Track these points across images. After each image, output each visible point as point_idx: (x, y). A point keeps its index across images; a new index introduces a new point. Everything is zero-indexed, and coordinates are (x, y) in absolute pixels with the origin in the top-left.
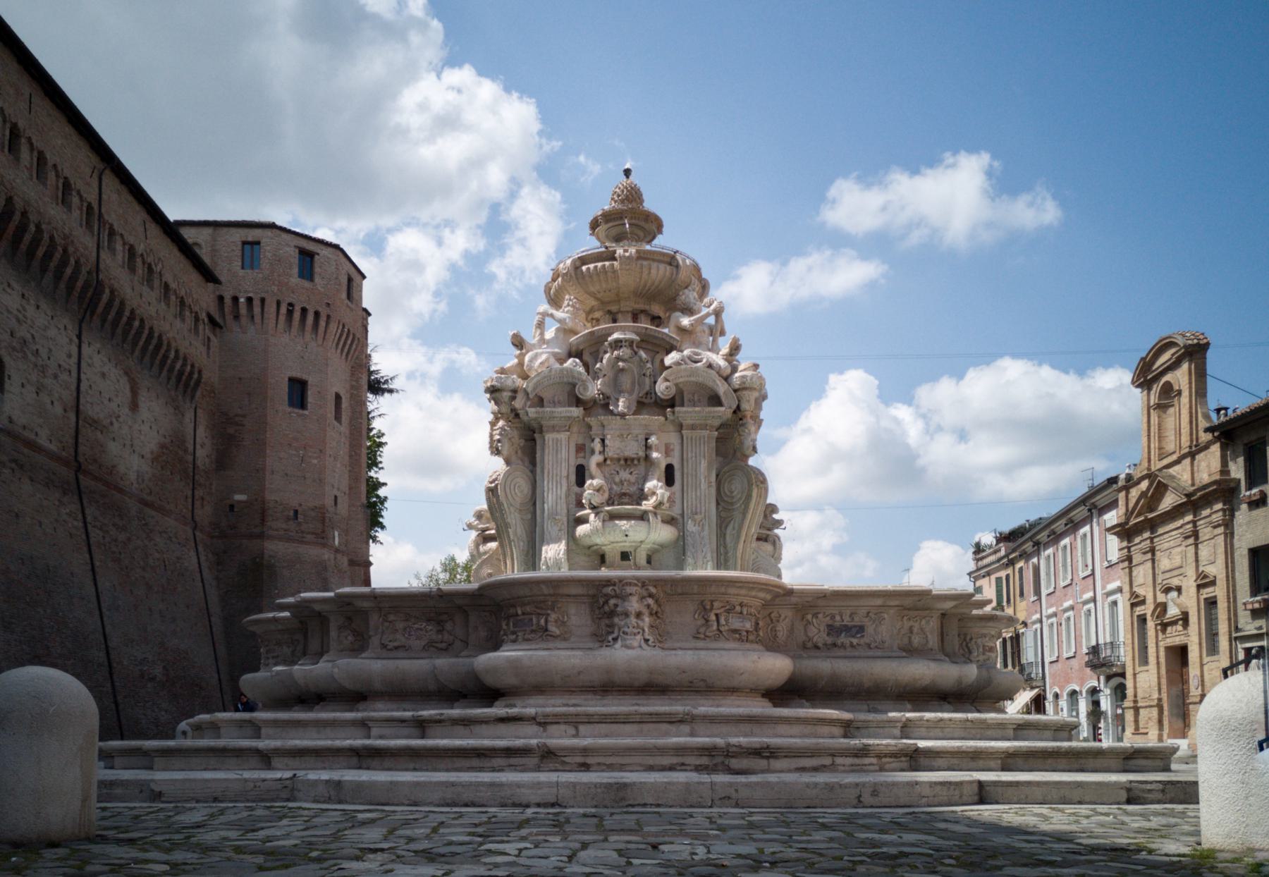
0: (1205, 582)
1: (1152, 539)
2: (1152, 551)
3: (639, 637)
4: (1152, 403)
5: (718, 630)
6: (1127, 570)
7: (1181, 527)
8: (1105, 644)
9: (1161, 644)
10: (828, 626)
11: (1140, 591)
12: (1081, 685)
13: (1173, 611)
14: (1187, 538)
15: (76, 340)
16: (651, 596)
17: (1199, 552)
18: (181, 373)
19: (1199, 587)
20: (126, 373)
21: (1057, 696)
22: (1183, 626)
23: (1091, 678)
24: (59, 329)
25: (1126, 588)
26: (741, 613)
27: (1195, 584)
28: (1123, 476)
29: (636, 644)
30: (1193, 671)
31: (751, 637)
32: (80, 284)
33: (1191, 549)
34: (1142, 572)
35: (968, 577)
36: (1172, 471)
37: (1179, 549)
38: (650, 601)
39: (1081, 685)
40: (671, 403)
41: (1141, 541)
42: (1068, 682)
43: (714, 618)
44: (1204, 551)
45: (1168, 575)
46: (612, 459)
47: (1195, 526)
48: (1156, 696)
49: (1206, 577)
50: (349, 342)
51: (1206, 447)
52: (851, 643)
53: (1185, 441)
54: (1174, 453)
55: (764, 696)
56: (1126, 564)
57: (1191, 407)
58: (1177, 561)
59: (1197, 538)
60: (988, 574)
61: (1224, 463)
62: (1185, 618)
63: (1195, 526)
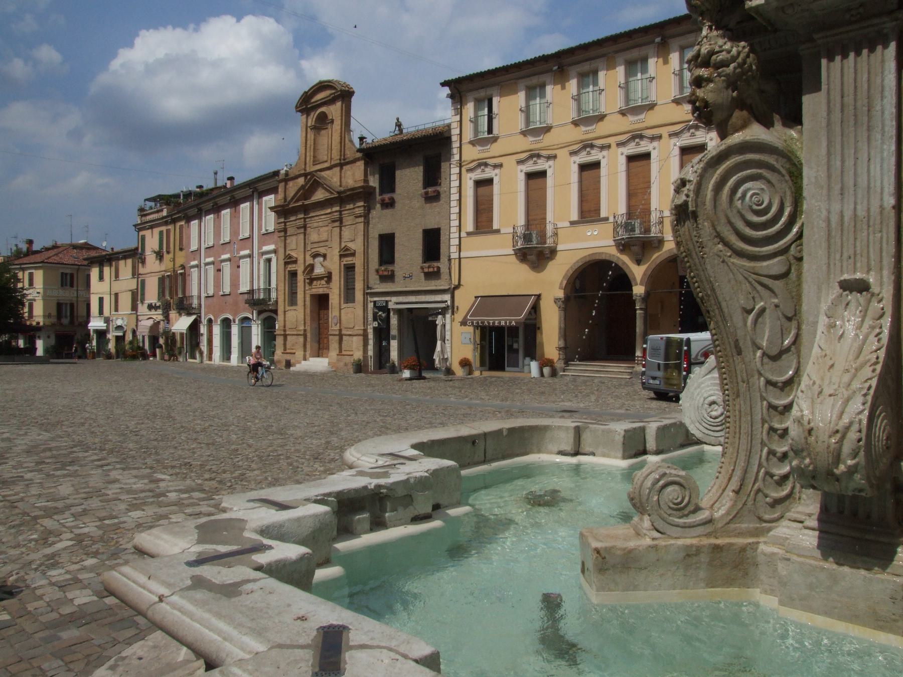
0: (346, 253)
1: (305, 219)
2: (305, 227)
4: (309, 124)
6: (283, 238)
7: (330, 213)
8: (259, 289)
9: (307, 292)
11: (294, 254)
12: (235, 315)
13: (319, 270)
14: (334, 221)
17: (342, 233)
19: (341, 256)
21: (210, 321)
22: (326, 282)
23: (244, 310)
25: (281, 251)
27: (338, 254)
28: (283, 172)
30: (333, 312)
33: (338, 230)
34: (294, 242)
35: (134, 228)
36: (323, 174)
37: (326, 229)
39: (235, 315)
41: (295, 221)
42: (223, 311)
44: (347, 233)
45: (315, 245)
47: (341, 214)
48: (302, 328)
49: (347, 250)
51: (354, 161)
53: (336, 155)
54: (326, 161)
56: (282, 234)
57: (341, 133)
58: (324, 236)
59: (341, 222)
60: (152, 227)
61: (366, 175)
62: (329, 277)
63: (341, 214)
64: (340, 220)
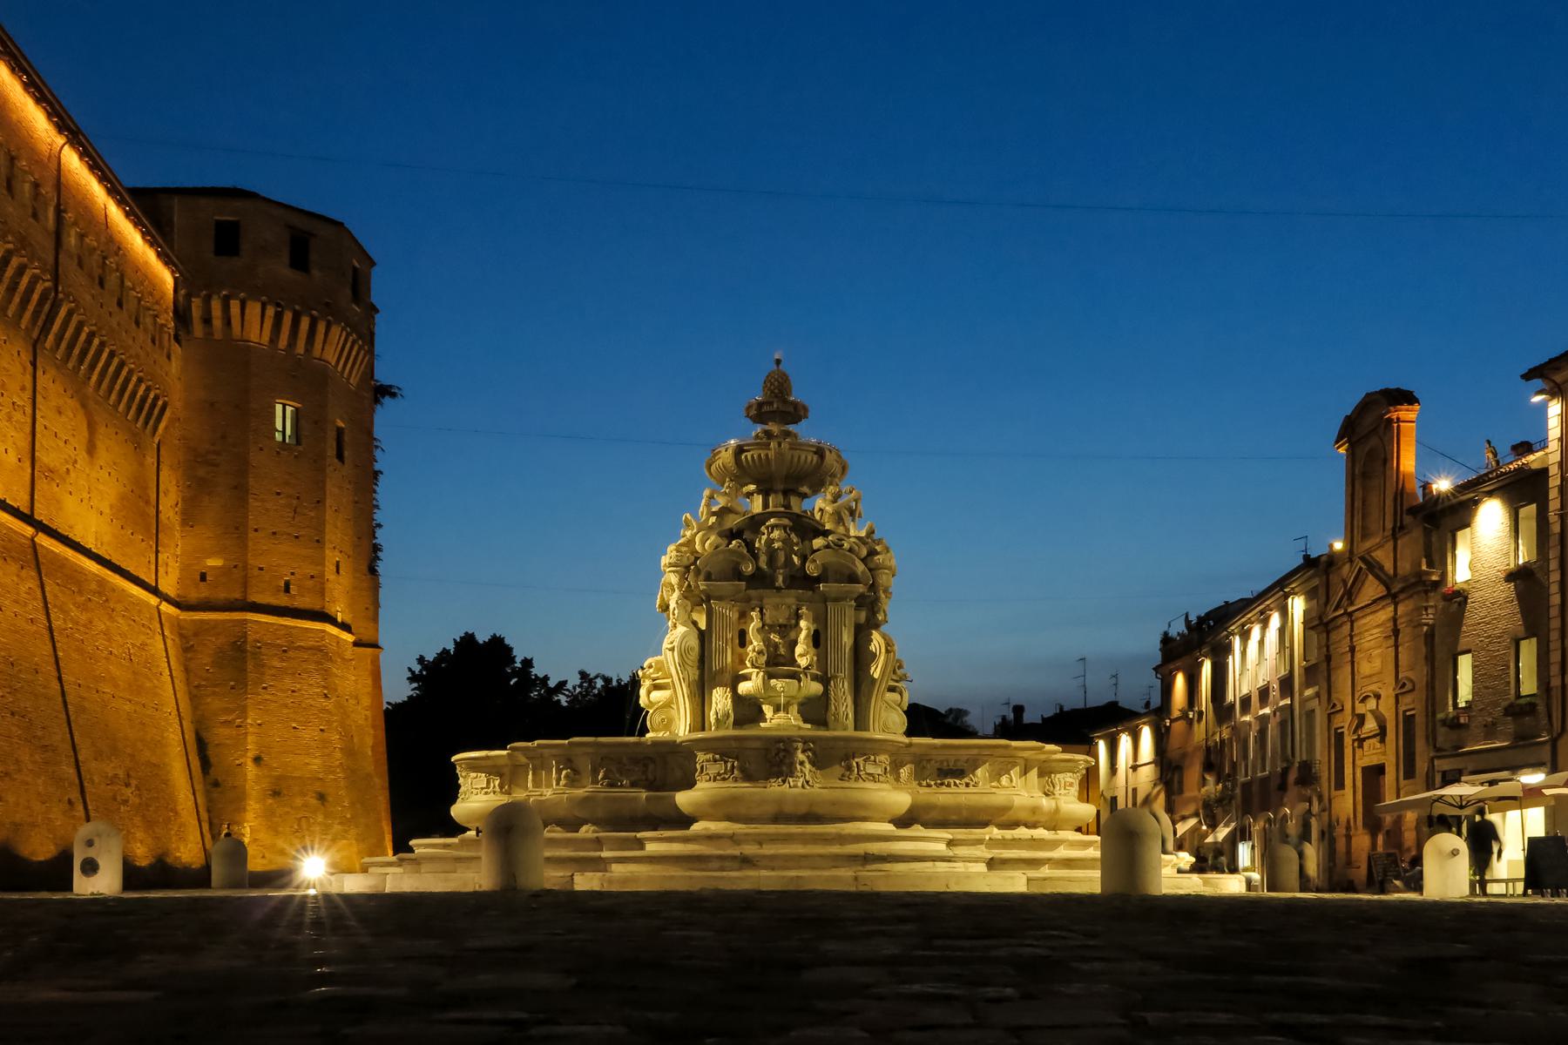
3: (801, 779)
5: (858, 774)
10: (938, 769)
15: (30, 368)
16: (810, 750)
18: (144, 400)
20: (84, 406)
24: (13, 355)
25: (1324, 697)
26: (875, 761)
29: (800, 784)
31: (881, 778)
32: (36, 297)
38: (810, 754)
40: (818, 580)
43: (855, 764)
46: (769, 626)
50: (354, 353)
52: (955, 782)
55: (889, 822)
64: (1396, 632)
